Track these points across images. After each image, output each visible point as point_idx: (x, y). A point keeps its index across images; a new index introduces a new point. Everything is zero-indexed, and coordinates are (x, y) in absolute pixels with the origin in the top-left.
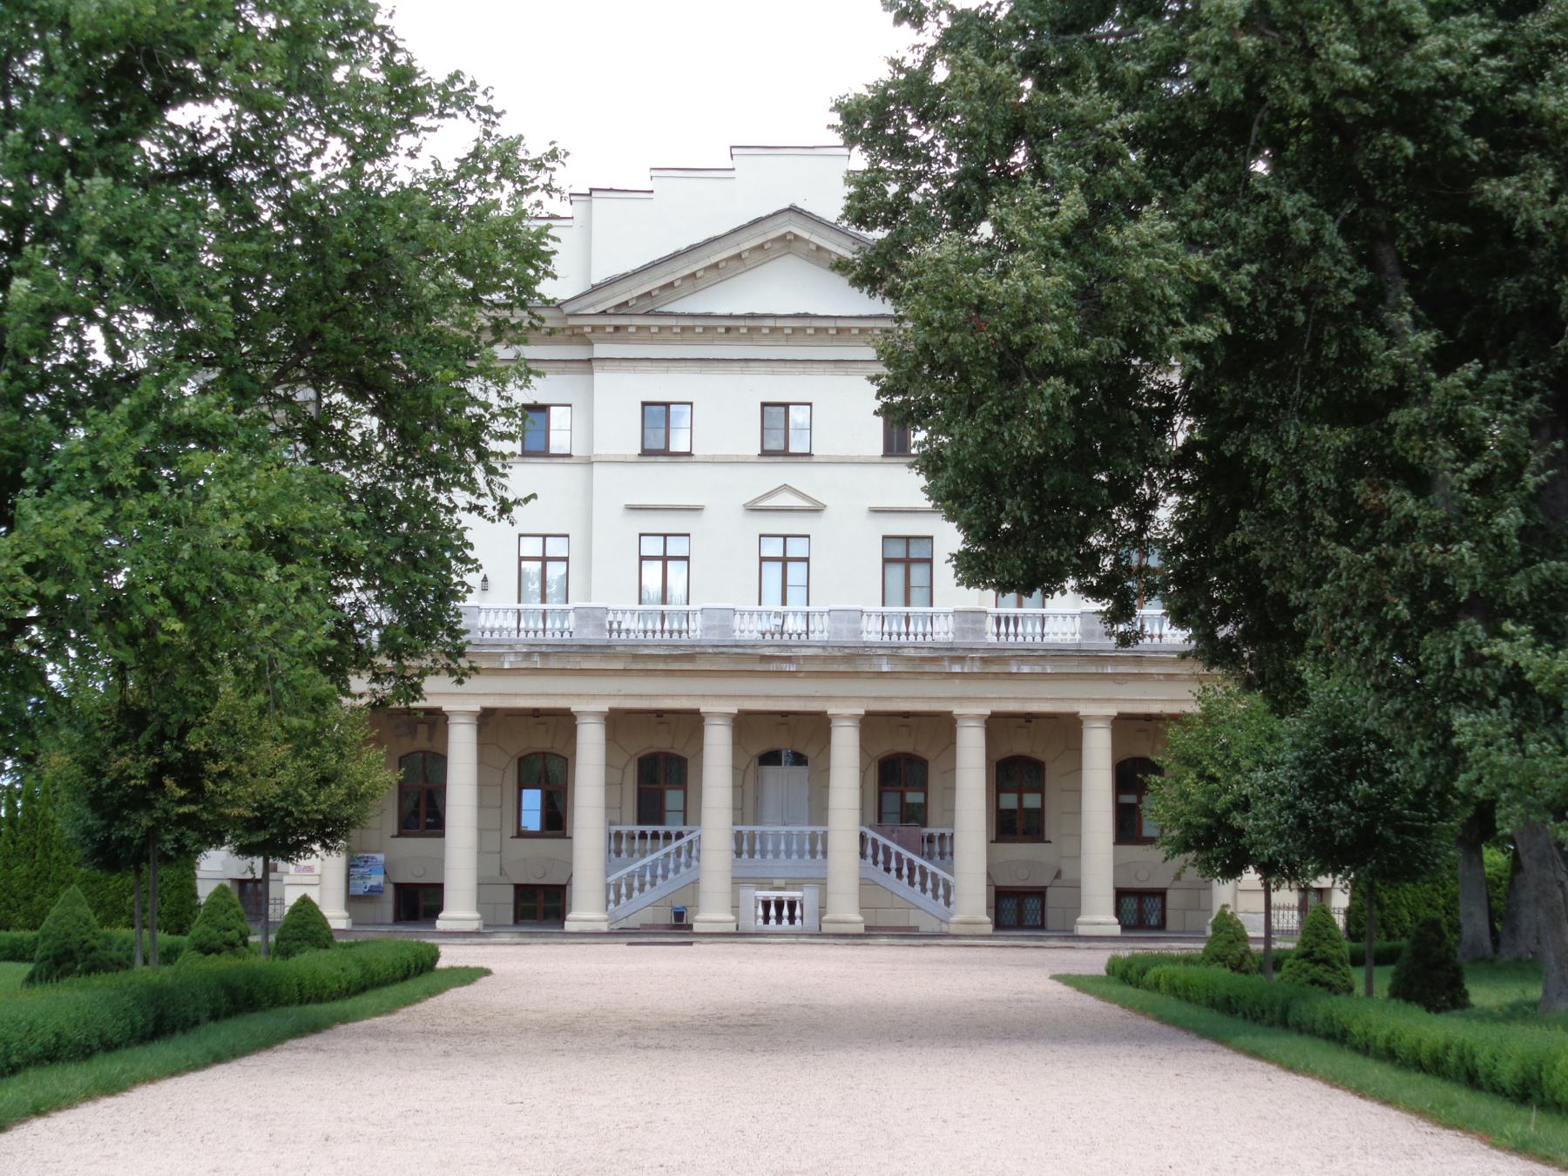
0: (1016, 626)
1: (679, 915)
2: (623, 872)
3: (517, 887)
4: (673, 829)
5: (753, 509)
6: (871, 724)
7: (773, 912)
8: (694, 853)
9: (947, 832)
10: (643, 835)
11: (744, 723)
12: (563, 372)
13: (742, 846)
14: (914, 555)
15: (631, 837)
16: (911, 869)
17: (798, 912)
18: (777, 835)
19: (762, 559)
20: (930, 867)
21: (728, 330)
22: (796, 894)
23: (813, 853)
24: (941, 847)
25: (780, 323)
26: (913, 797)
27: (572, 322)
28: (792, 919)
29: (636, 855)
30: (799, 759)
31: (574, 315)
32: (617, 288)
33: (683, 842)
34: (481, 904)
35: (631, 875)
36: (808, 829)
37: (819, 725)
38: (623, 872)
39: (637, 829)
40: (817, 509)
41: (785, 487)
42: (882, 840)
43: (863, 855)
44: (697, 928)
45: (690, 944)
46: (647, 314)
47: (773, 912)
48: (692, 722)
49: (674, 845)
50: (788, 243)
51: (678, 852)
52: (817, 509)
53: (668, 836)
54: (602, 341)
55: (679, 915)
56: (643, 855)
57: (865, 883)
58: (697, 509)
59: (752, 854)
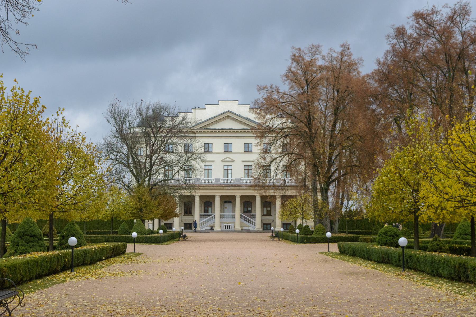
1: (212, 227)
2: (202, 221)
3: (184, 224)
4: (210, 214)
5: (222, 161)
6: (242, 197)
7: (227, 227)
10: (205, 215)
11: (222, 197)
13: (221, 217)
14: (249, 168)
15: (203, 215)
16: (249, 220)
18: (227, 215)
19: (224, 169)
20: (252, 220)
21: (218, 131)
22: (230, 224)
23: (233, 218)
24: (253, 216)
25: (227, 130)
26: (249, 209)
27: (193, 130)
28: (230, 228)
30: (230, 202)
31: (193, 129)
32: (200, 125)
33: (212, 216)
35: (203, 222)
36: (232, 214)
37: (234, 197)
38: (202, 221)
39: (204, 214)
40: (233, 161)
41: (228, 157)
42: (244, 216)
43: (241, 218)
44: (214, 230)
46: (205, 129)
47: (227, 227)
48: (213, 197)
49: (210, 217)
50: (228, 117)
51: (211, 218)
52: (233, 161)
53: (209, 215)
54: (198, 133)
55: (212, 227)
56: (205, 218)
57: (241, 223)
58: (213, 161)
59: (223, 218)
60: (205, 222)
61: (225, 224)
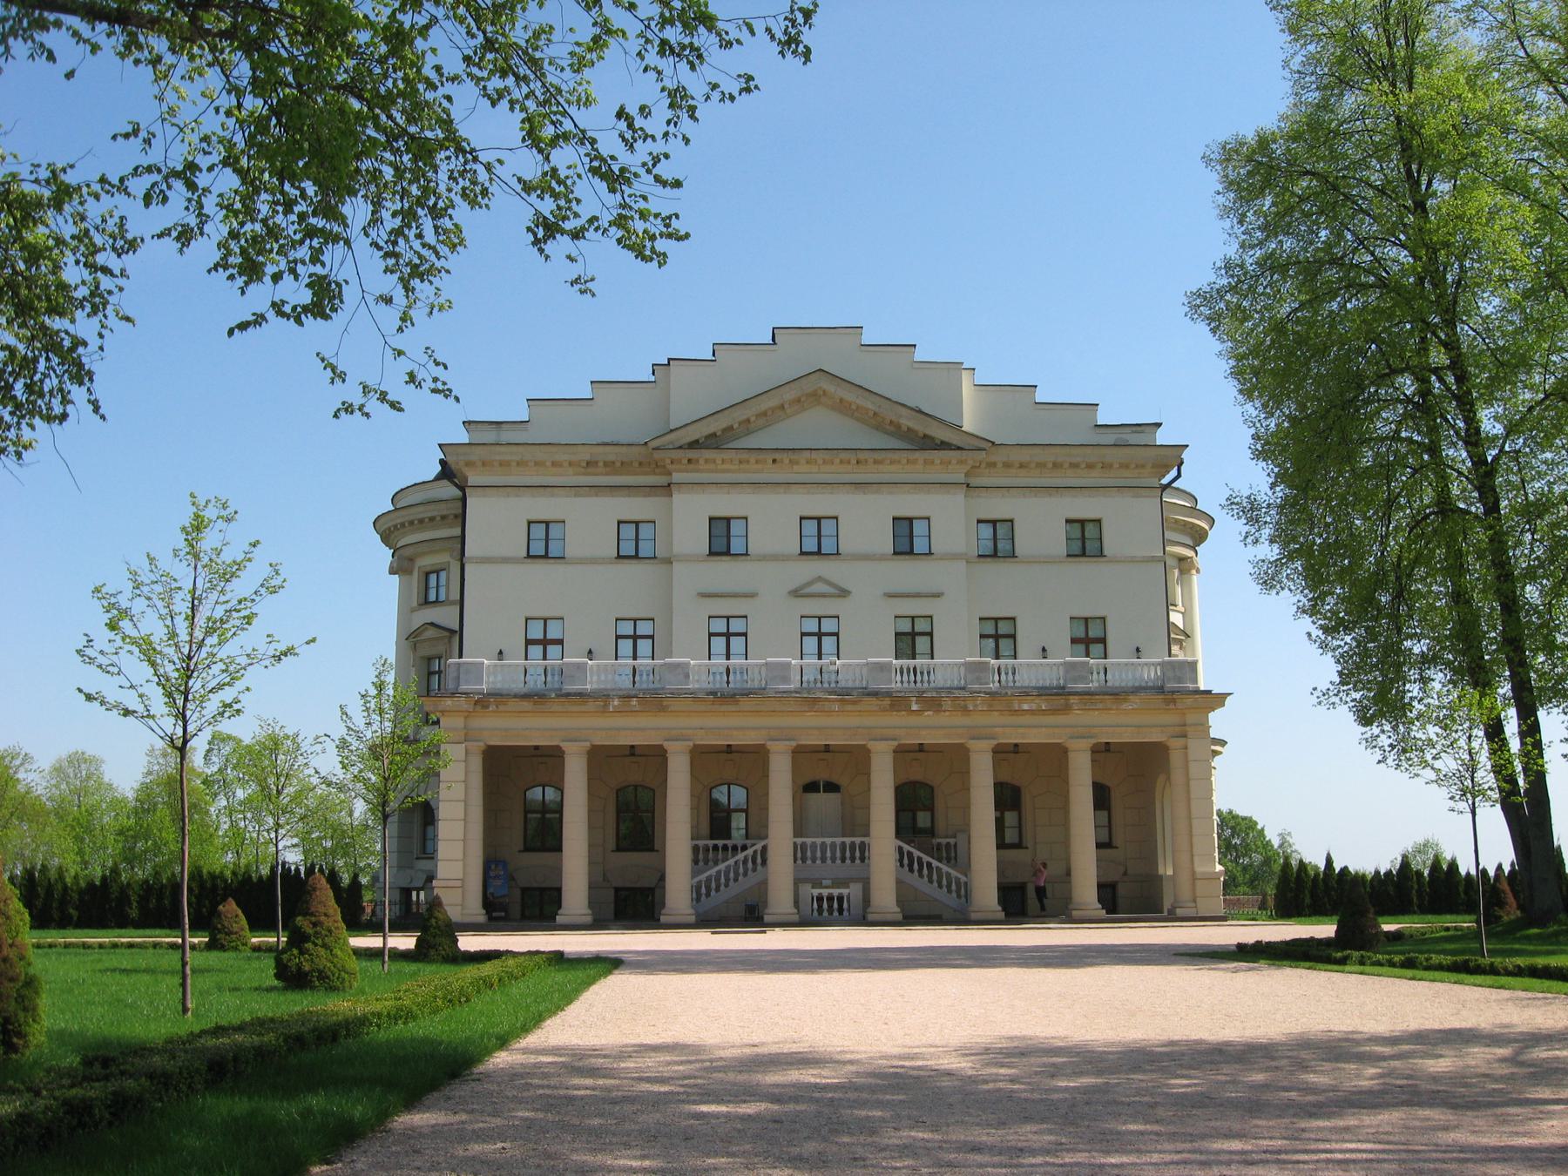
0: (1014, 674)
2: (703, 877)
3: (617, 890)
5: (796, 593)
8: (759, 860)
9: (952, 841)
10: (716, 848)
12: (649, 495)
15: (707, 849)
17: (845, 905)
22: (845, 892)
29: (711, 863)
33: (750, 852)
34: (592, 903)
35: (709, 879)
38: (703, 877)
39: (711, 843)
40: (843, 593)
41: (820, 579)
42: (906, 847)
44: (767, 918)
45: (764, 932)
49: (741, 856)
50: (816, 397)
51: (745, 861)
52: (843, 593)
56: (716, 863)
60: (718, 879)
61: (816, 892)
